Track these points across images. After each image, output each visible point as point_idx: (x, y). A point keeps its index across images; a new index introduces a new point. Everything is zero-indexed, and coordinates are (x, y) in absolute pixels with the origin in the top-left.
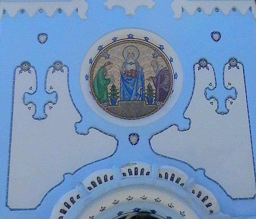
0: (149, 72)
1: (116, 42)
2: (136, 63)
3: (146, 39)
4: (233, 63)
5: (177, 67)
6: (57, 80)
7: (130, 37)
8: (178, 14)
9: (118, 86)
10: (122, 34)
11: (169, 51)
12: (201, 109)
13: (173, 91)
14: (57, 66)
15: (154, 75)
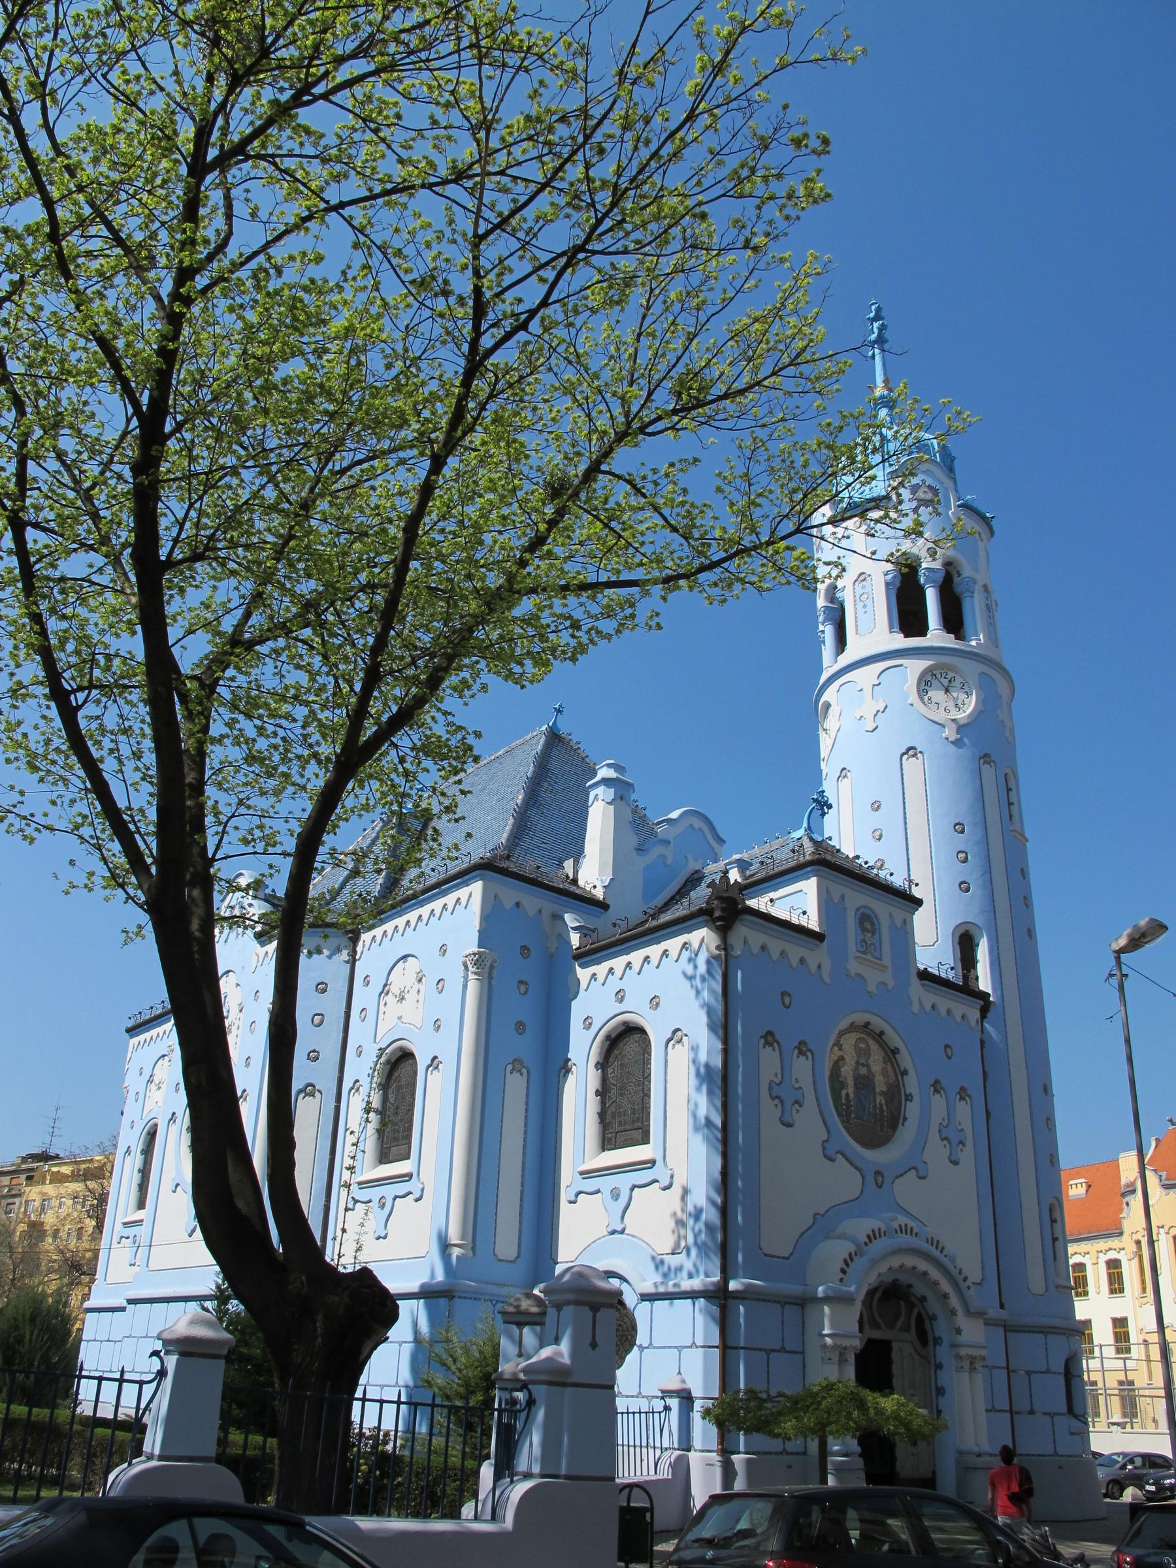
0: (880, 1084)
1: (853, 1028)
2: (868, 1066)
3: (882, 1033)
4: (963, 1093)
5: (911, 1084)
6: (801, 1068)
7: (867, 1025)
8: (915, 1008)
9: (852, 1096)
10: (860, 1018)
11: (905, 1060)
12: (936, 1153)
13: (905, 1119)
14: (802, 1048)
15: (885, 1089)
